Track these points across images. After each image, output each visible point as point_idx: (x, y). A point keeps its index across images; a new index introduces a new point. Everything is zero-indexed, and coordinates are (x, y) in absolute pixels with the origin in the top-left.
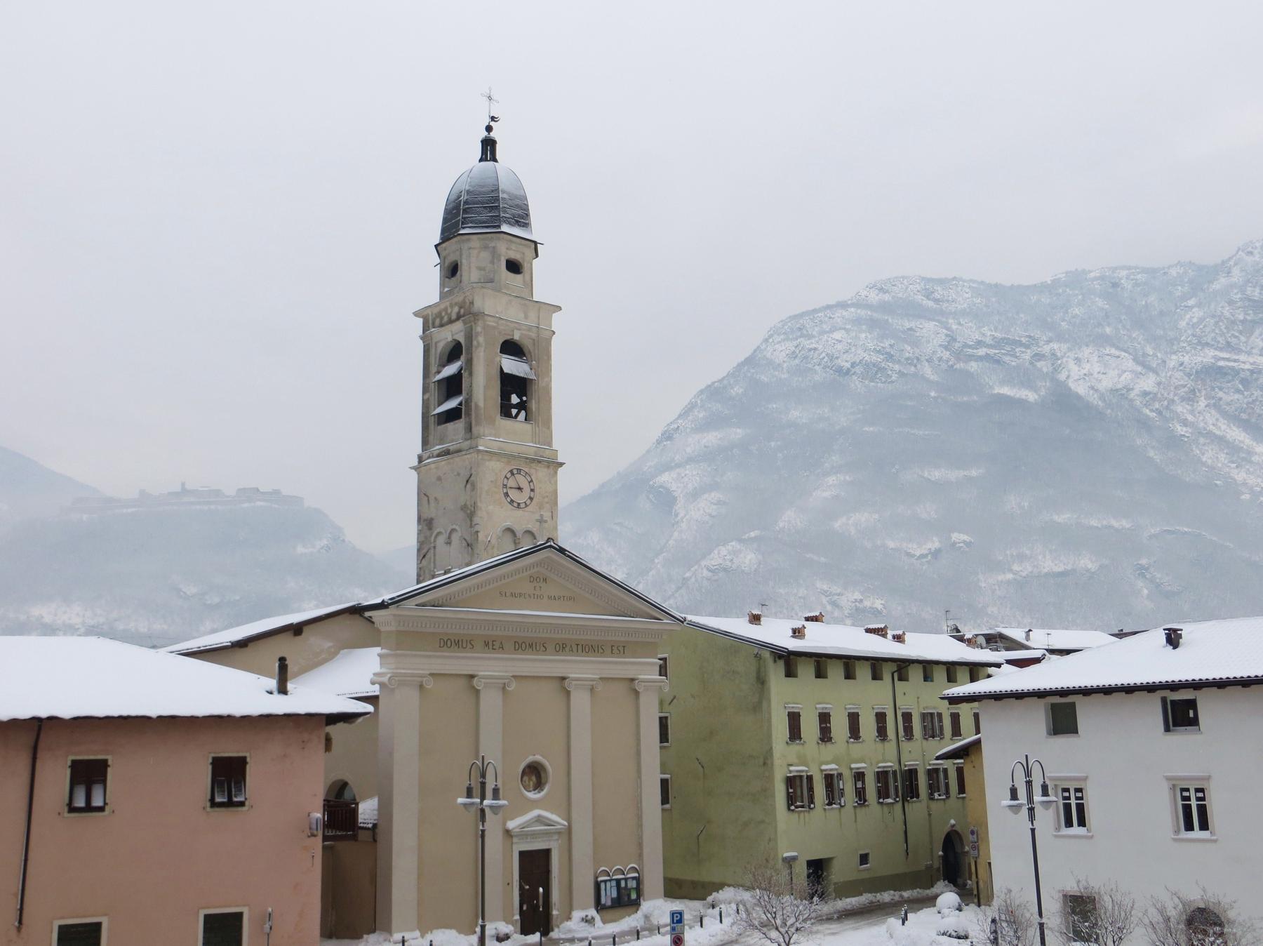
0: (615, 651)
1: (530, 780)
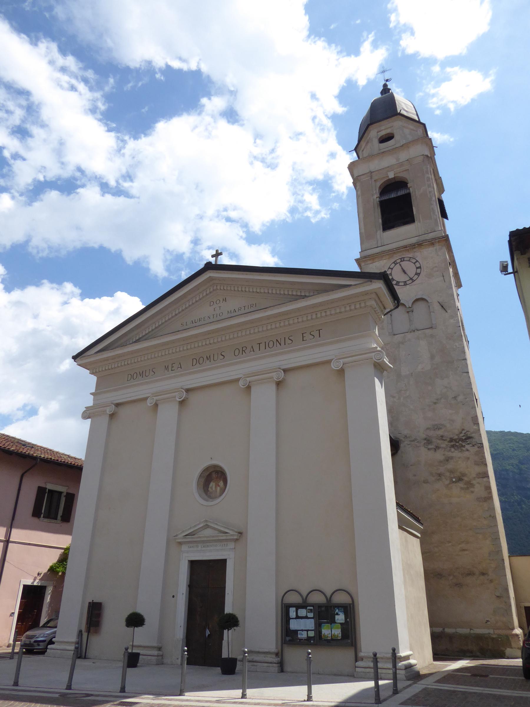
0: (307, 336)
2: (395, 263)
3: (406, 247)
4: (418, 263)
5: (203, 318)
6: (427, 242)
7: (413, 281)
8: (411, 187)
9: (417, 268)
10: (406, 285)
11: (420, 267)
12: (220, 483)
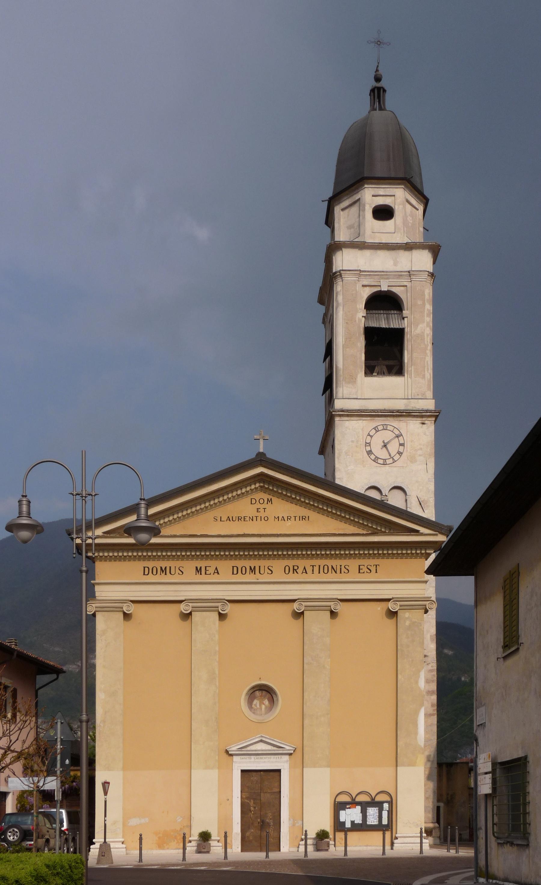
1: (261, 703)
5: (243, 518)
7: (394, 461)
12: (265, 701)
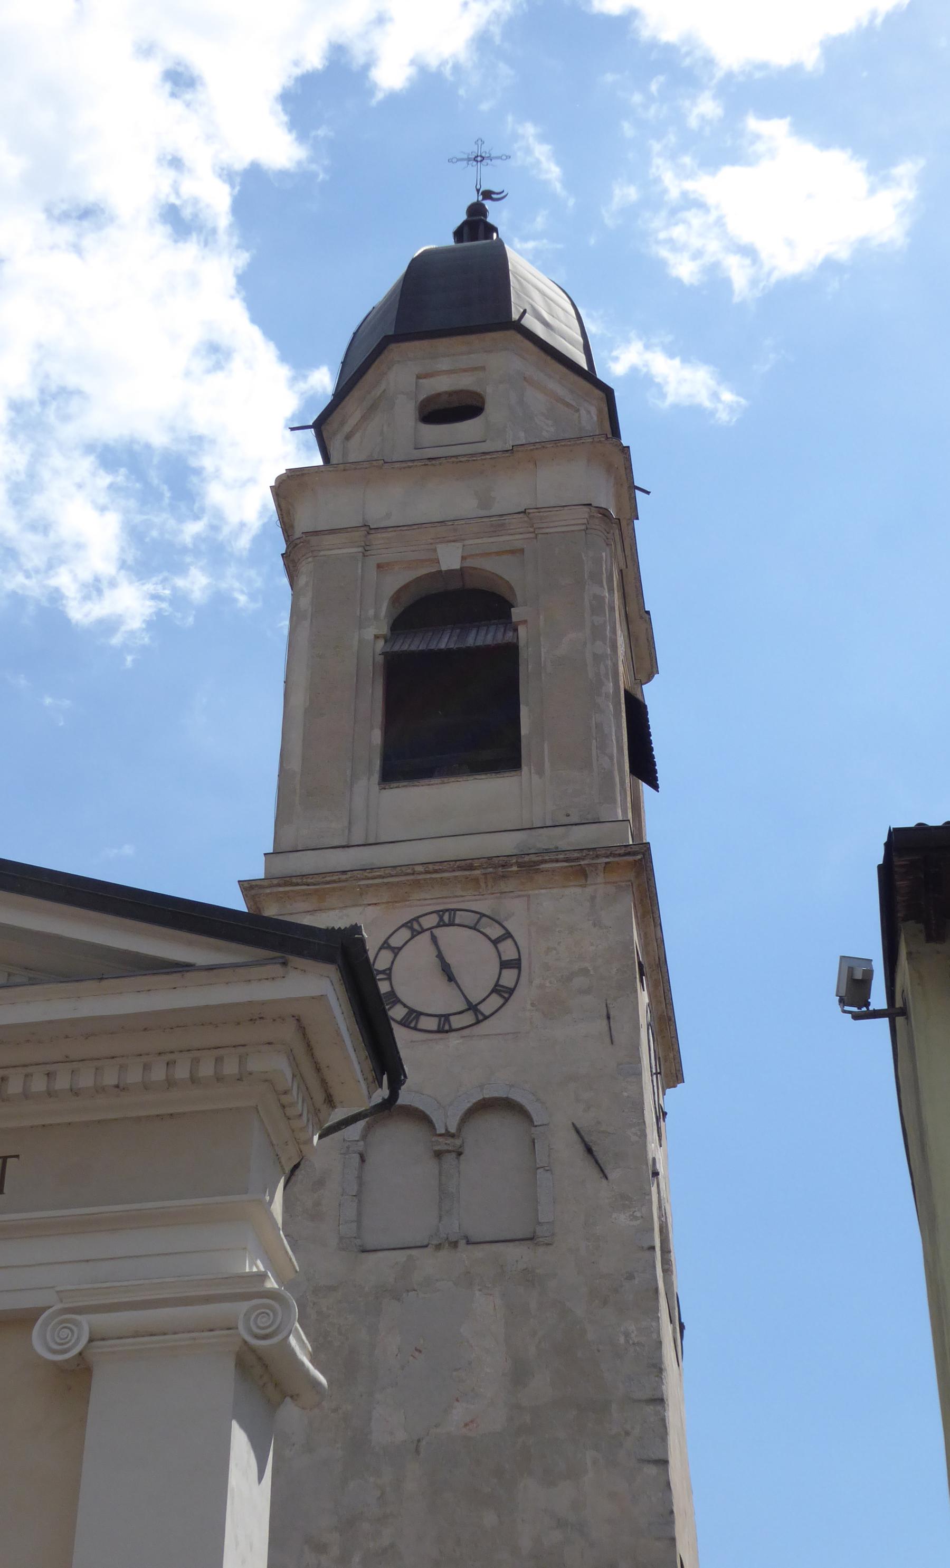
2: (414, 927)
3: (471, 868)
4: (509, 942)
6: (557, 861)
8: (525, 622)
9: (505, 965)
10: (447, 1032)
11: (515, 964)
